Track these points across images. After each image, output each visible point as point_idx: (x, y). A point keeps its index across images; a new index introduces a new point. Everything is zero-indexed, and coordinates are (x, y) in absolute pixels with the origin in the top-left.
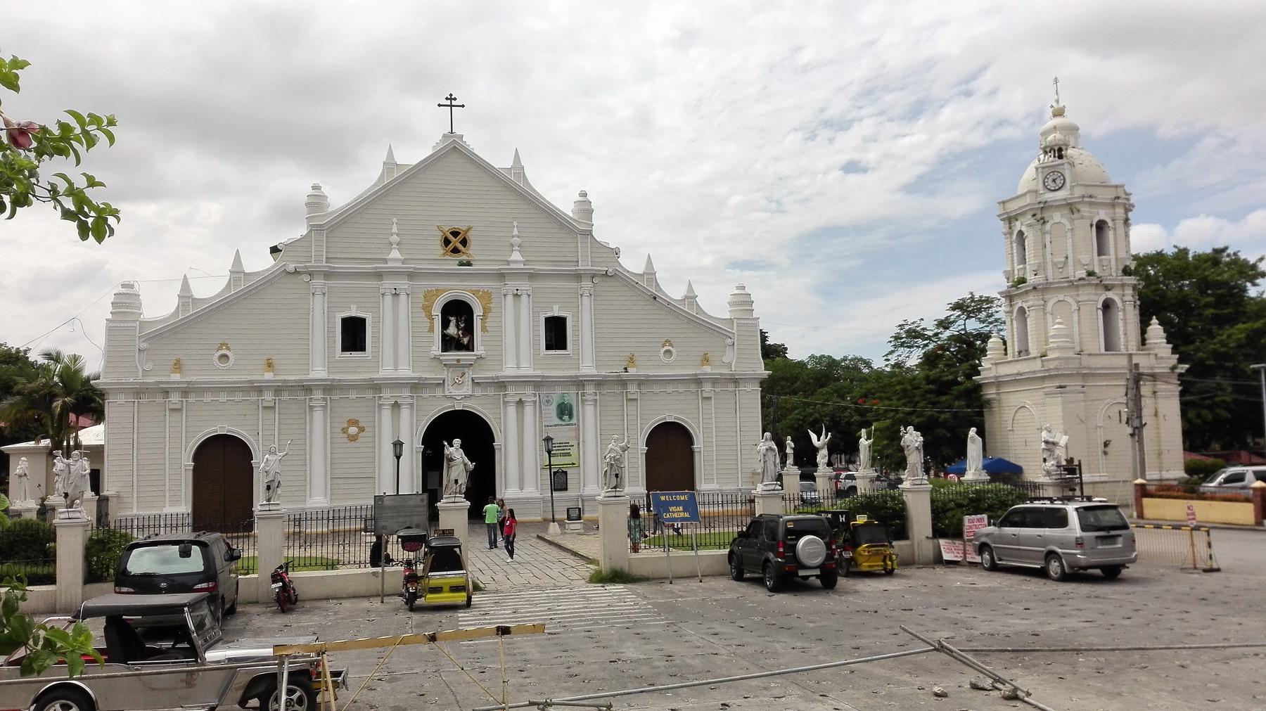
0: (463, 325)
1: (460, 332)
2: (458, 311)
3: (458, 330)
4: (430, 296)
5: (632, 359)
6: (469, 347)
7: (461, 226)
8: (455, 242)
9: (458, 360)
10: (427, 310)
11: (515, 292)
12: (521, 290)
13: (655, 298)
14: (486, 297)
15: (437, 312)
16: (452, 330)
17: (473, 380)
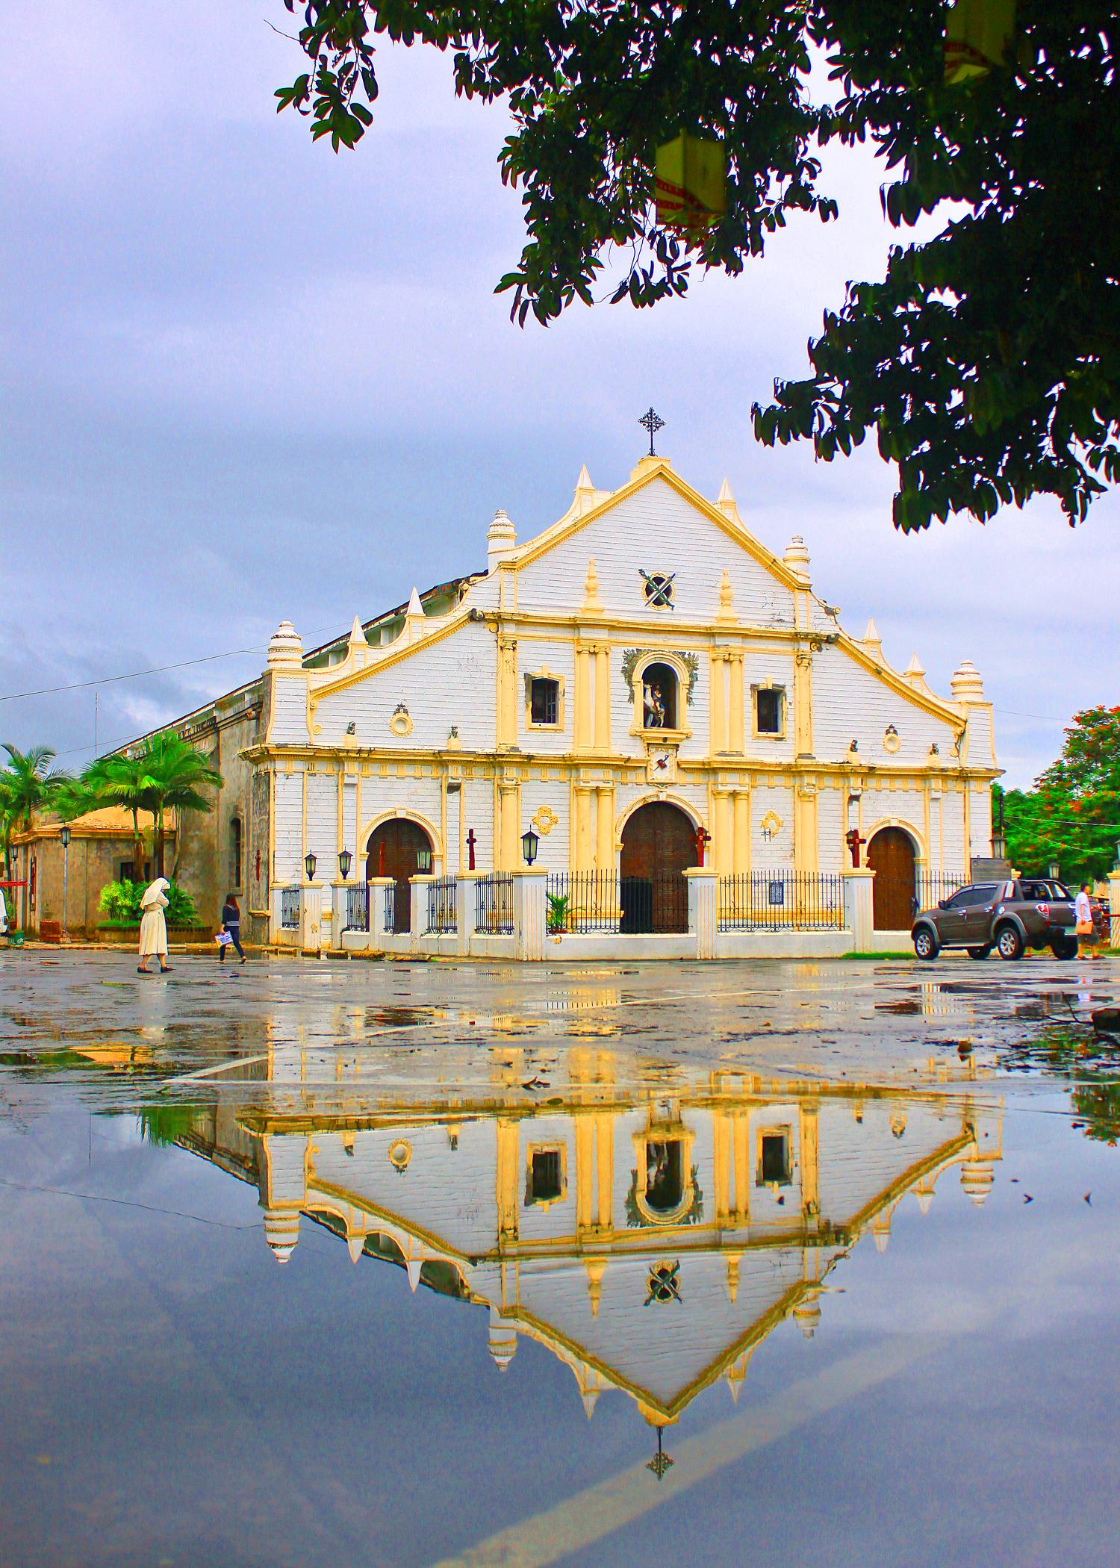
0: (659, 696)
1: (658, 704)
2: (660, 678)
3: (655, 702)
4: (631, 659)
5: (854, 746)
6: (670, 723)
7: (666, 576)
8: (659, 590)
9: (665, 739)
10: (628, 673)
11: (727, 657)
12: (734, 655)
13: (879, 673)
14: (692, 665)
15: (638, 675)
16: (650, 702)
17: (678, 765)
